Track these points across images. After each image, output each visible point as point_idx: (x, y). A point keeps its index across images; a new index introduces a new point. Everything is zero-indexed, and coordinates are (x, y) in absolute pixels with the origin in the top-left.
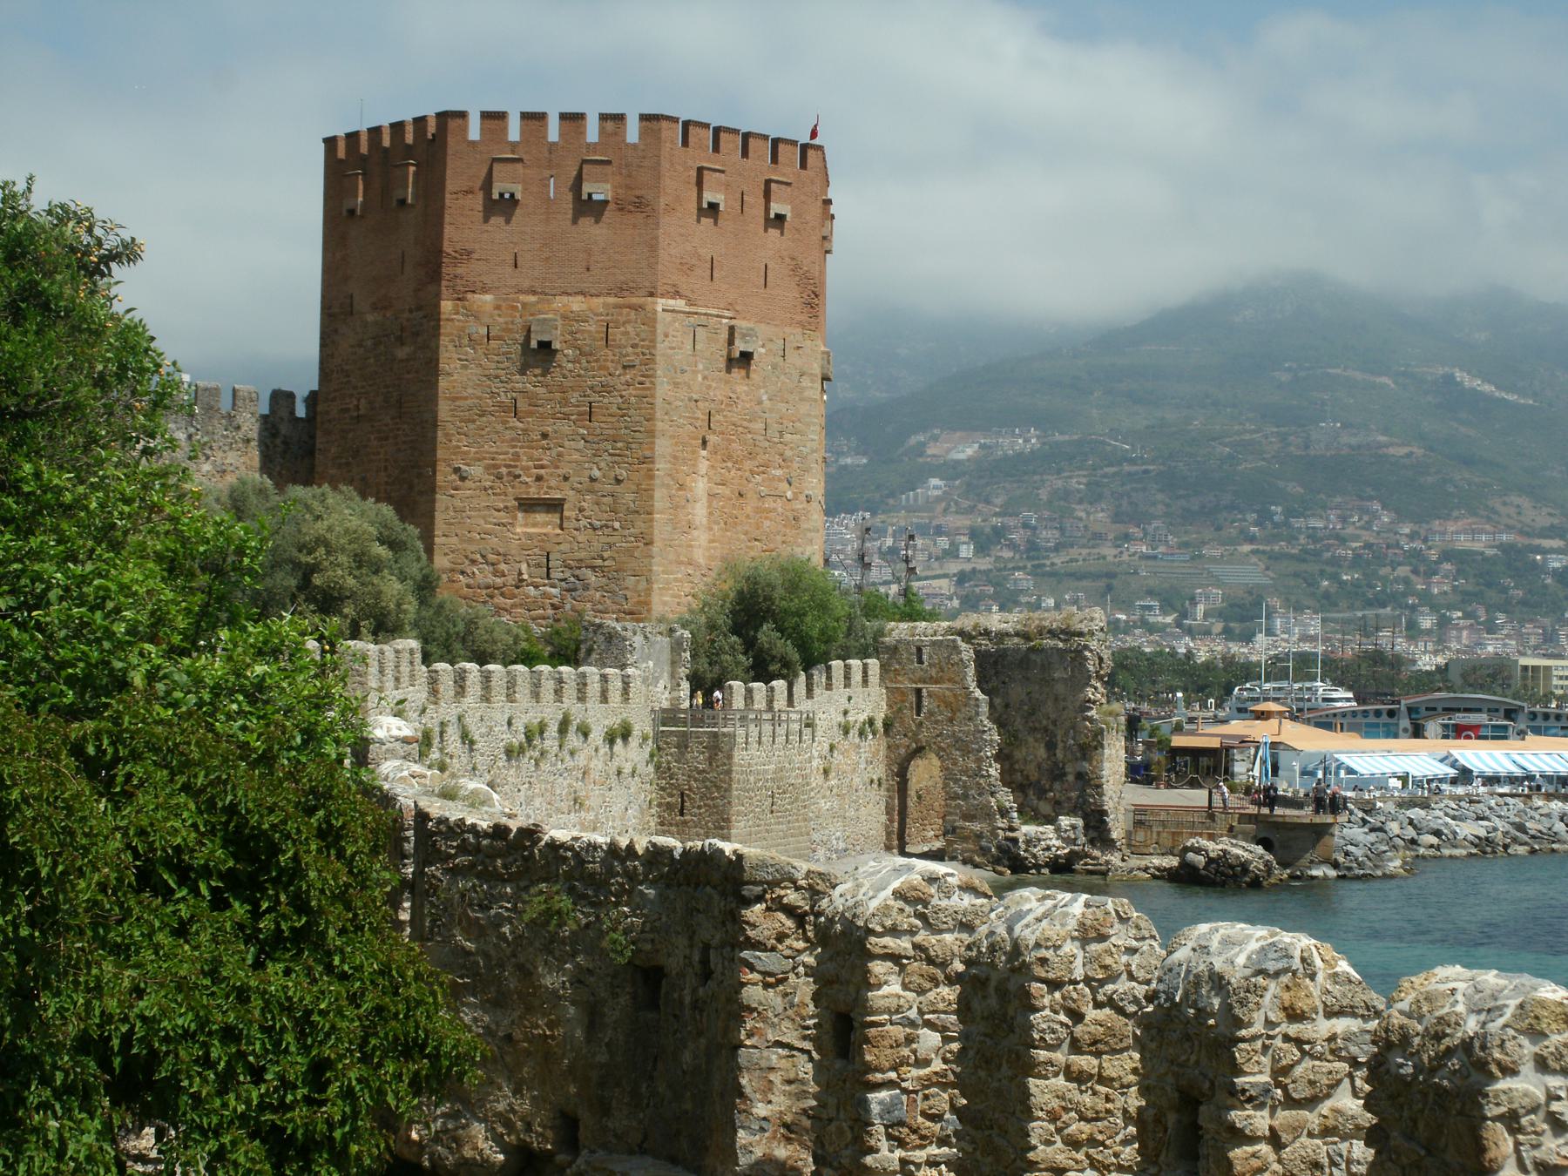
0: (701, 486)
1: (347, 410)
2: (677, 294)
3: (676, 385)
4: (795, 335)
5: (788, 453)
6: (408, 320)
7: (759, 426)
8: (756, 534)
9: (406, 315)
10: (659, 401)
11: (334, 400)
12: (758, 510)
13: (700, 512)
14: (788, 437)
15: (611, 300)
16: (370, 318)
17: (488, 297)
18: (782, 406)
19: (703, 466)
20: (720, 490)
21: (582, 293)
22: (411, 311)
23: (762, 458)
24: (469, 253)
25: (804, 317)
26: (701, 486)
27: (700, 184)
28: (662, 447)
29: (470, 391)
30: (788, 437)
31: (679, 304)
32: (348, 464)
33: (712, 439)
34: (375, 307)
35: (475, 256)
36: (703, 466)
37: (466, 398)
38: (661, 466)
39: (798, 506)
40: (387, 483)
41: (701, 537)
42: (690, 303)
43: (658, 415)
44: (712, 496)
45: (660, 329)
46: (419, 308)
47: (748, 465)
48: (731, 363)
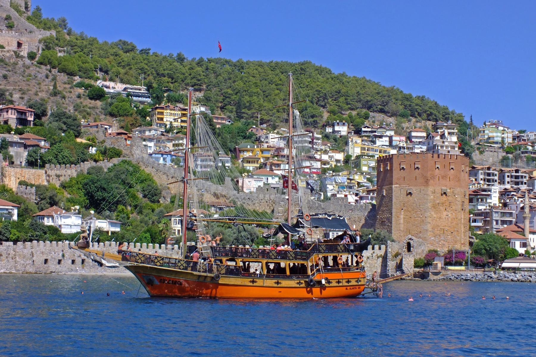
0: (402, 217)
2: (397, 184)
3: (397, 200)
4: (423, 188)
5: (421, 209)
7: (415, 205)
8: (414, 224)
10: (393, 203)
12: (414, 220)
13: (402, 221)
14: (421, 206)
18: (420, 201)
19: (403, 213)
20: (406, 217)
23: (415, 211)
25: (425, 184)
26: (402, 217)
27: (400, 164)
28: (394, 211)
30: (421, 206)
31: (398, 186)
33: (404, 208)
36: (403, 213)
38: (394, 214)
39: (423, 218)
41: (402, 226)
42: (400, 185)
43: (393, 205)
44: (404, 218)
45: (393, 190)
47: (412, 212)
48: (407, 195)
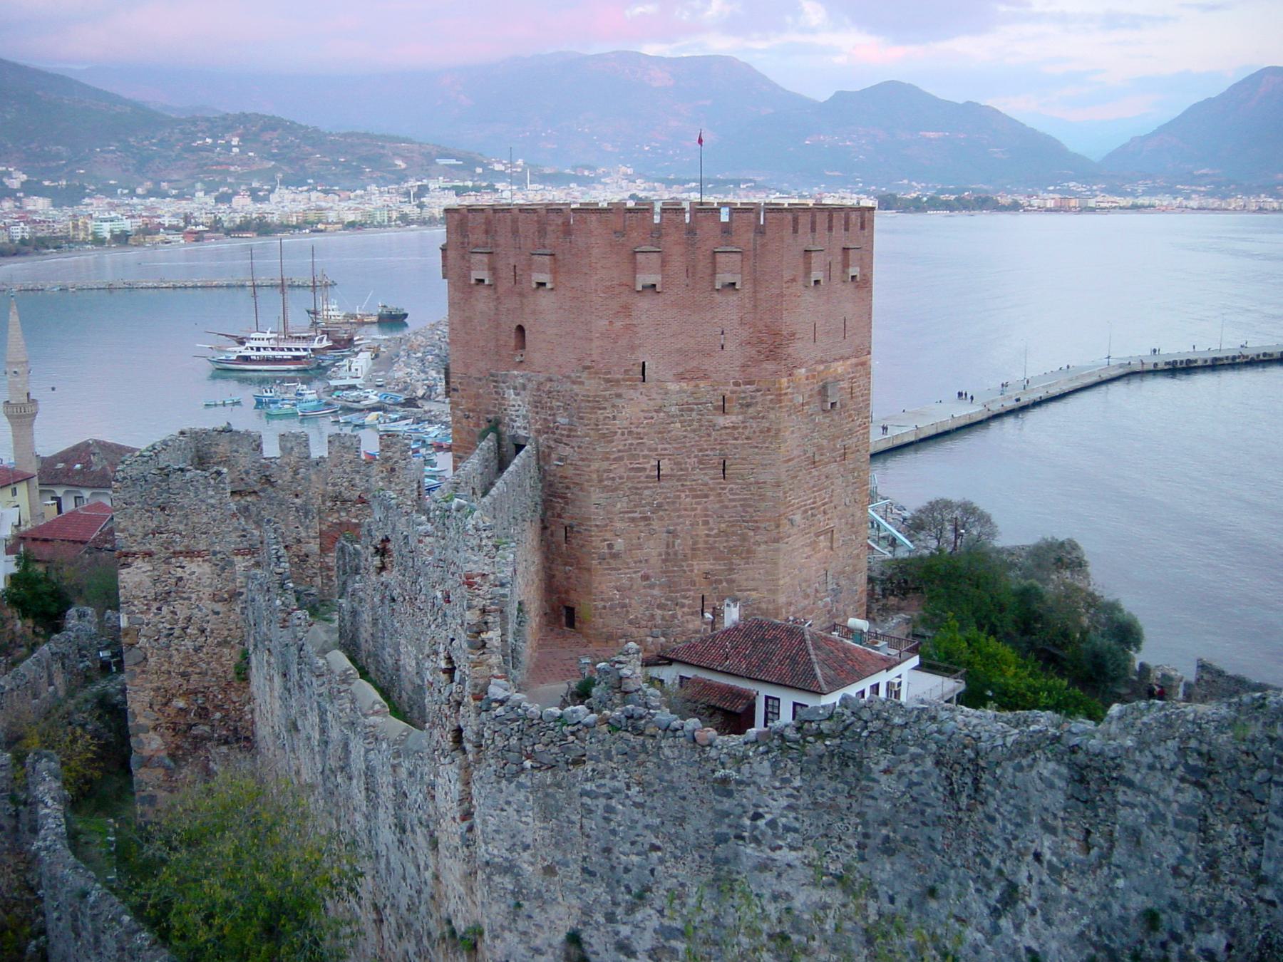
1: (645, 469)
6: (733, 392)
9: (732, 387)
11: (621, 459)
15: (854, 361)
16: (673, 387)
17: (803, 370)
21: (842, 358)
22: (737, 384)
24: (793, 335)
29: (795, 452)
32: (646, 519)
34: (681, 377)
35: (797, 336)
37: (792, 459)
40: (708, 536)
46: (750, 383)
